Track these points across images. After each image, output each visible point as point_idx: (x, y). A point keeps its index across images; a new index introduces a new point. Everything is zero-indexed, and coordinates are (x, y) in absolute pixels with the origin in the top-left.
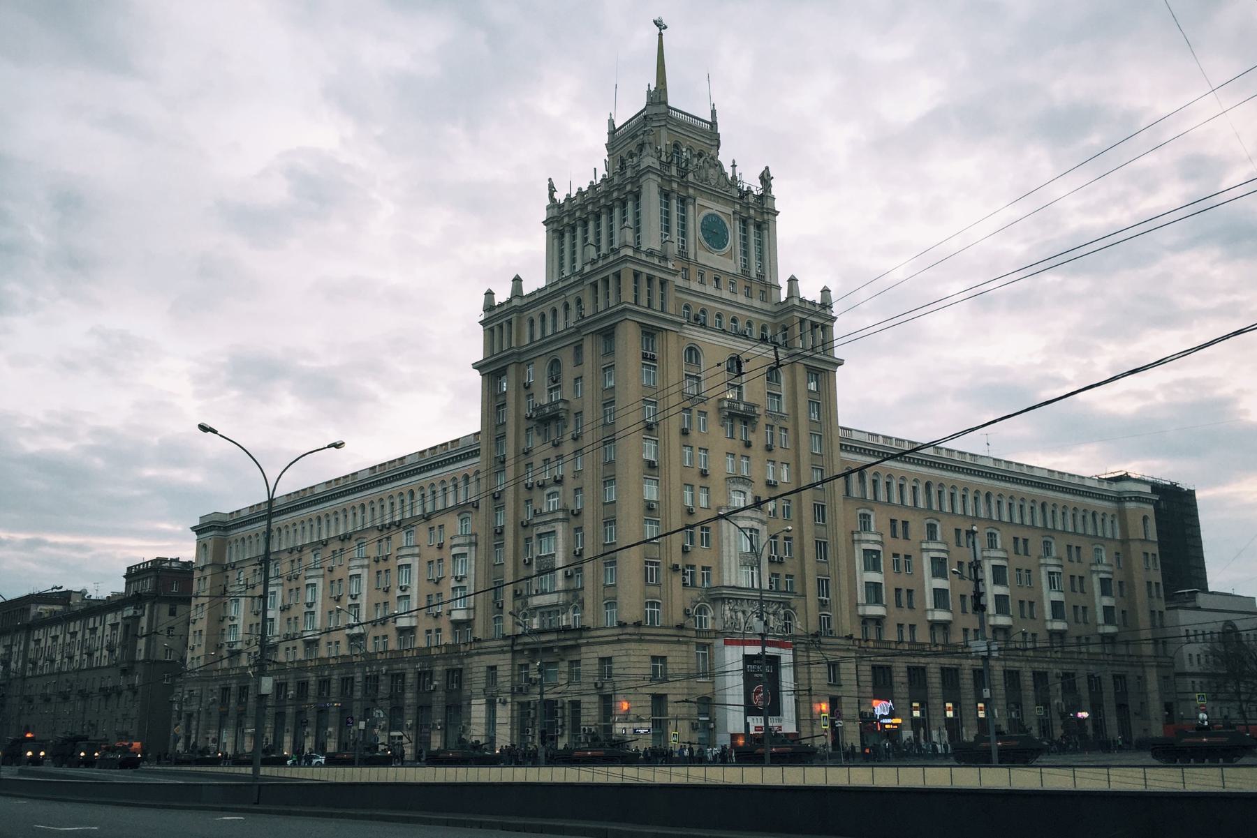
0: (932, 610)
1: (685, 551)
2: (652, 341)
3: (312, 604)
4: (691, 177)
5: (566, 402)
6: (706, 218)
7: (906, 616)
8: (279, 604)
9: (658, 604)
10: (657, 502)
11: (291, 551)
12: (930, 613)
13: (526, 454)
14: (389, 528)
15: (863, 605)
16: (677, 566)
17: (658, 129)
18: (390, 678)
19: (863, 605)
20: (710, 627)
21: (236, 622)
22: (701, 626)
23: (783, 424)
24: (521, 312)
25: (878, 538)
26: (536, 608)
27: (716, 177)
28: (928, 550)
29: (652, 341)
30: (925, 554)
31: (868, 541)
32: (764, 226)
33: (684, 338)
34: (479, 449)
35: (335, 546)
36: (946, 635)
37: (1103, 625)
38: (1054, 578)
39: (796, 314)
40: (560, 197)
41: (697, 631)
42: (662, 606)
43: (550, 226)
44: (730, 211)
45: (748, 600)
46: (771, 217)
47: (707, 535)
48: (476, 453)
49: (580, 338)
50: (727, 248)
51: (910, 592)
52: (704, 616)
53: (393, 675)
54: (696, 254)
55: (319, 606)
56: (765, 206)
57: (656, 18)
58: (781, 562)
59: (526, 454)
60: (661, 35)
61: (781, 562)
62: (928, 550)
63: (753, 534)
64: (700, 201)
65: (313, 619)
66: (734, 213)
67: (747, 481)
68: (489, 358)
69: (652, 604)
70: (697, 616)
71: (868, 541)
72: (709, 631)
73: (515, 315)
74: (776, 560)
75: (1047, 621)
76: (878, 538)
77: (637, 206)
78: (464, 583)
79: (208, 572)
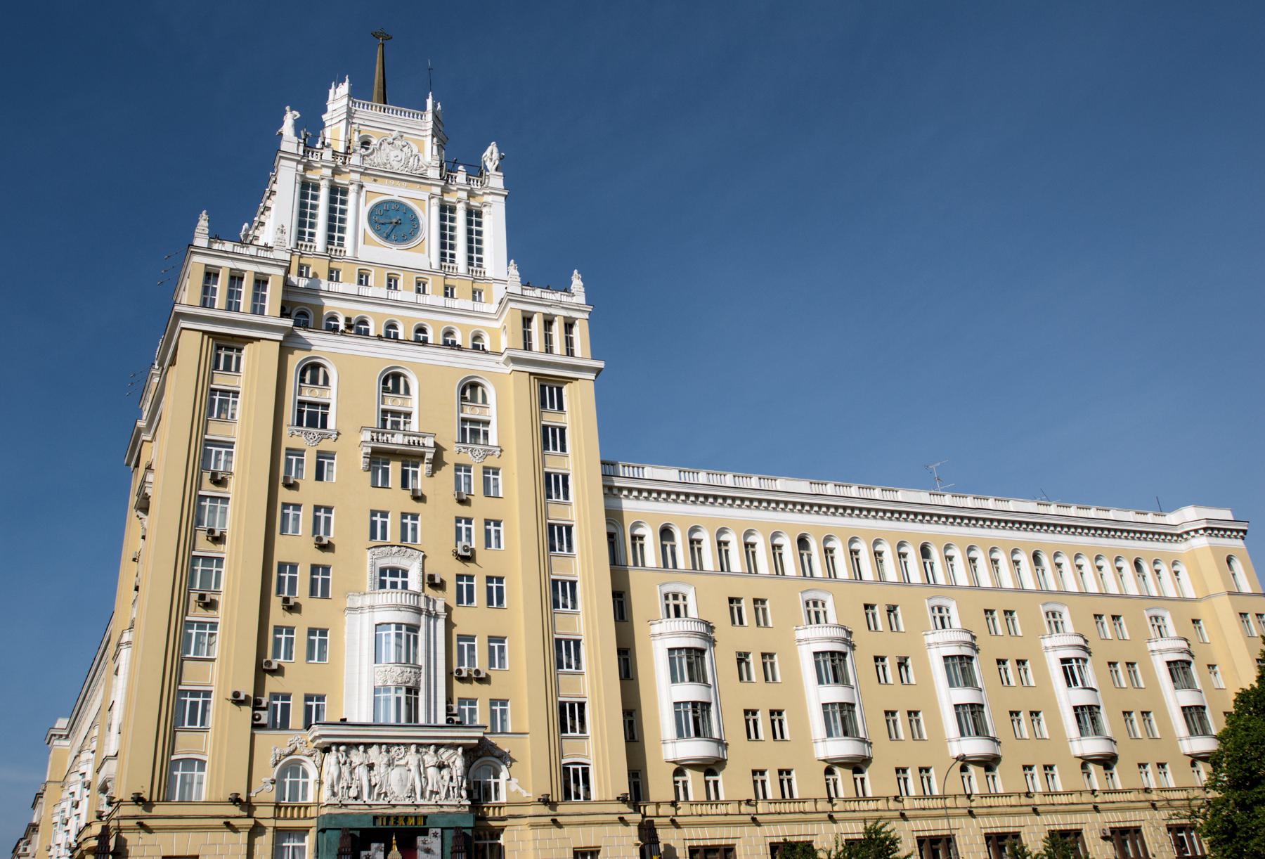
7: (768, 755)
20: (311, 798)
45: (380, 745)
51: (776, 713)
52: (301, 780)
64: (369, 185)
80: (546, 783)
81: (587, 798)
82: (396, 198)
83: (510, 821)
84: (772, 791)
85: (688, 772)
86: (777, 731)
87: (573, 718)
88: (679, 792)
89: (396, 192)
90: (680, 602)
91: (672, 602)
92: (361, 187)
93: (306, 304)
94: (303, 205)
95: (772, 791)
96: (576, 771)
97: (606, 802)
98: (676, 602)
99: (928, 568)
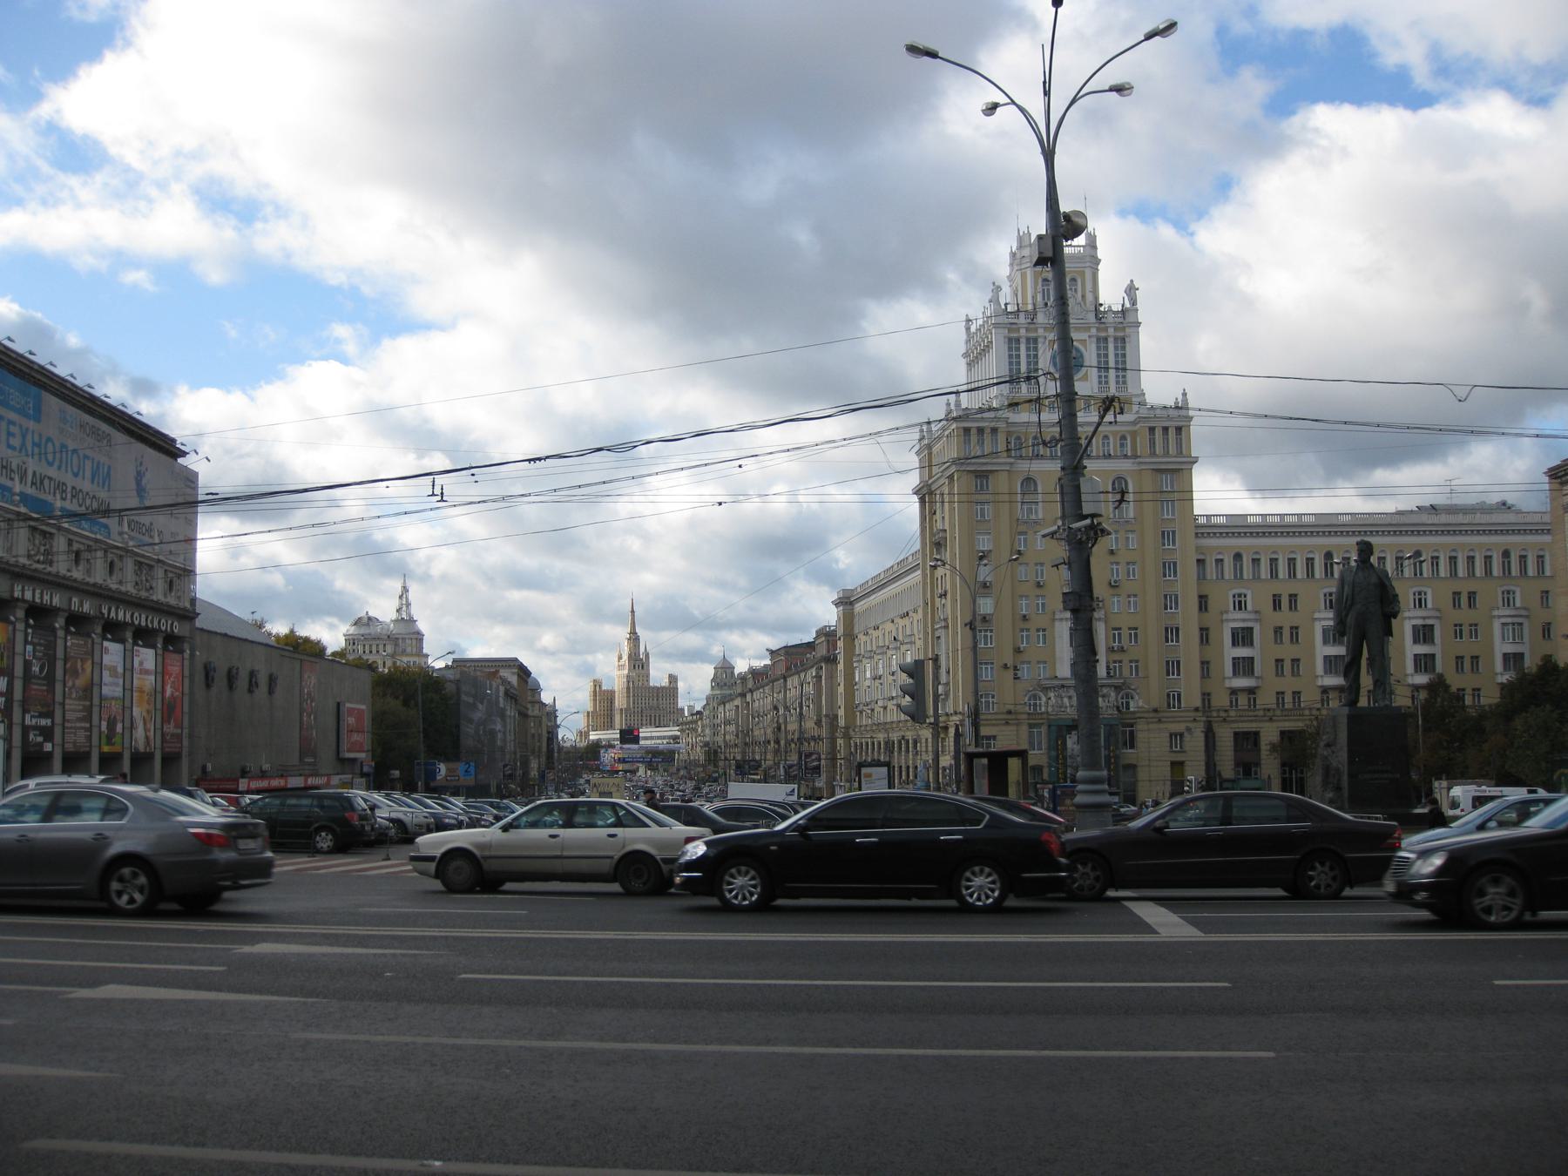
0: (1322, 676)
2: (987, 482)
15: (1229, 678)
16: (1006, 665)
19: (1229, 678)
22: (1035, 709)
25: (1252, 616)
28: (1320, 619)
29: (987, 482)
31: (1234, 620)
32: (1126, 339)
41: (1029, 714)
56: (1127, 321)
58: (1122, 650)
61: (1122, 650)
66: (1090, 337)
71: (1234, 620)
75: (1497, 674)
76: (1252, 616)
81: (1179, 708)
83: (1138, 720)
86: (1295, 672)
88: (1234, 704)
91: (1237, 599)
94: (1010, 356)
96: (1174, 695)
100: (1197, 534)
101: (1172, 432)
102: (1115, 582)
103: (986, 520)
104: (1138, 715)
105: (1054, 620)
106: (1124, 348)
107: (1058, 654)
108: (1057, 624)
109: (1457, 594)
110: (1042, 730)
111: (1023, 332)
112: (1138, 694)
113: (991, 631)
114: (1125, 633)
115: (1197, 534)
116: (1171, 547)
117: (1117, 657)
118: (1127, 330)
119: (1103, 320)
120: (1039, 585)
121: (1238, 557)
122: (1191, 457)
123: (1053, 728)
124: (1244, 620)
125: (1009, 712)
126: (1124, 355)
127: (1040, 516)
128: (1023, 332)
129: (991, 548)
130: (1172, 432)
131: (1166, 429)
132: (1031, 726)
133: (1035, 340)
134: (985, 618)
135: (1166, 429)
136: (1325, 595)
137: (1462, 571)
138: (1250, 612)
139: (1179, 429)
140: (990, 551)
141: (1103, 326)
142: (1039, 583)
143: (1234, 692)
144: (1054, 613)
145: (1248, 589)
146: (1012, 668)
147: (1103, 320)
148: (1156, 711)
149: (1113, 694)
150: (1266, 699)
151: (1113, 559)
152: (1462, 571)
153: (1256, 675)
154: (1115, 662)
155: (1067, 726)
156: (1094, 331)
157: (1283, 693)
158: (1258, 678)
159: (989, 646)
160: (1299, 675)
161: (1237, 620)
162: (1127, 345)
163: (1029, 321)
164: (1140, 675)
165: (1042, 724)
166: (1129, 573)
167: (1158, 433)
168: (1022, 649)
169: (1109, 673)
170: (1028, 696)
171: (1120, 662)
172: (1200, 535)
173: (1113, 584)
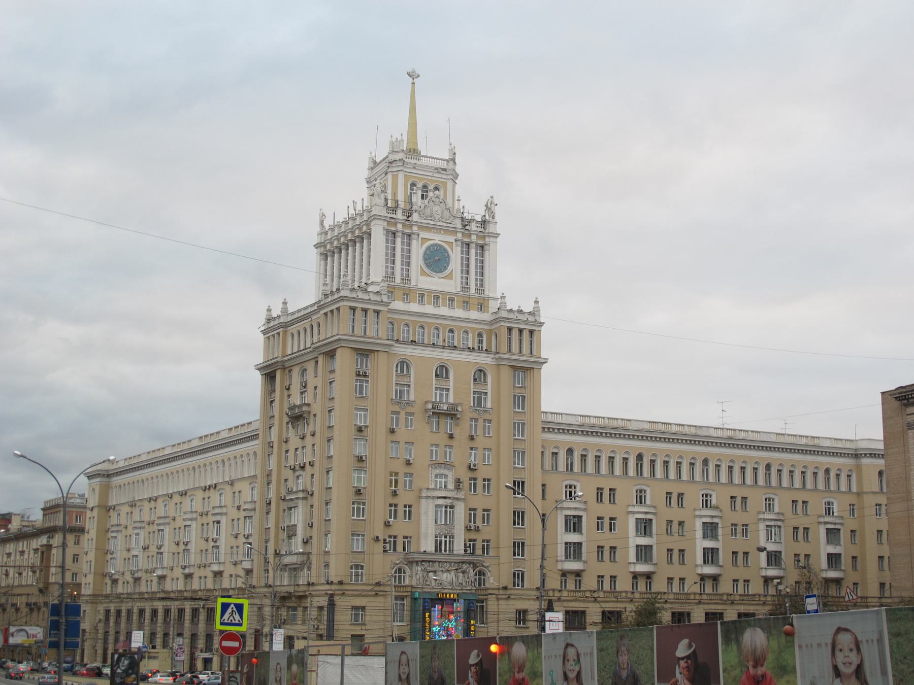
0: (634, 563)
1: (387, 525)
2: (367, 360)
3: (161, 546)
4: (415, 217)
5: (309, 405)
6: (428, 248)
7: (607, 569)
8: (142, 544)
9: (362, 567)
10: (364, 488)
11: (150, 500)
12: (632, 565)
13: (286, 442)
14: (209, 489)
16: (377, 537)
17: (396, 173)
18: (206, 610)
19: (561, 561)
20: (407, 582)
21: (114, 556)
23: (487, 417)
24: (287, 327)
25: (581, 506)
26: (286, 565)
27: (439, 212)
28: (633, 513)
29: (367, 360)
30: (630, 516)
31: (569, 508)
32: (486, 247)
33: (395, 354)
34: (258, 434)
35: (176, 498)
36: (649, 585)
37: (826, 571)
38: (771, 531)
39: (503, 324)
40: (328, 223)
42: (365, 568)
43: (319, 249)
44: (451, 239)
46: (492, 239)
47: (410, 511)
48: (255, 437)
49: (317, 356)
50: (447, 272)
53: (208, 609)
54: (417, 280)
55: (166, 550)
56: (487, 231)
57: (409, 70)
59: (286, 442)
60: (413, 83)
61: (477, 530)
62: (633, 513)
63: (448, 509)
64: (424, 235)
65: (162, 560)
66: (456, 240)
67: (448, 465)
68: (266, 362)
69: (357, 567)
70: (397, 575)
71: (569, 508)
72: (406, 586)
73: (281, 329)
74: (472, 528)
76: (581, 506)
77: (370, 244)
78: (250, 540)
79: (96, 511)
80: (506, 580)
81: (523, 586)
82: (437, 242)
83: (489, 596)
84: (607, 586)
85: (568, 575)
86: (613, 559)
87: (519, 549)
89: (437, 238)
90: (573, 490)
91: (568, 490)
92: (418, 235)
93: (393, 318)
95: (607, 586)
96: (518, 574)
97: (530, 589)
98: (570, 490)
99: (706, 472)
100: (544, 428)
101: (526, 334)
102: (475, 465)
103: (364, 398)
104: (490, 592)
105: (420, 497)
106: (482, 255)
107: (423, 530)
108: (423, 501)
109: (600, 491)
110: (405, 602)
111: (400, 226)
112: (490, 571)
113: (364, 504)
114: (479, 514)
115: (544, 428)
116: (520, 437)
117: (473, 536)
118: (487, 239)
119: (467, 227)
120: (408, 463)
121: (570, 451)
122: (540, 358)
123: (407, 602)
124: (835, 524)
125: (378, 584)
126: (482, 262)
127: (412, 398)
128: (400, 226)
129: (368, 424)
130: (526, 334)
131: (521, 331)
132: (397, 598)
133: (409, 235)
134: (359, 490)
135: (521, 331)
136: (637, 492)
137: (737, 479)
138: (836, 517)
139: (531, 332)
140: (367, 427)
141: (467, 232)
142: (409, 461)
143: (564, 574)
144: (421, 490)
145: (578, 481)
146: (382, 541)
147: (467, 227)
148: (505, 588)
149: (471, 570)
150: (589, 582)
151: (472, 444)
152: (737, 479)
153: (583, 559)
154: (470, 540)
155: (432, 599)
156: (459, 236)
157: (602, 577)
158: (584, 562)
159: (361, 518)
160: (615, 561)
161: (571, 508)
162: (486, 253)
163: (405, 218)
164: (491, 554)
165: (406, 596)
166: (484, 459)
167: (515, 333)
168: (391, 523)
169: (465, 551)
170: (395, 569)
171: (474, 540)
172: (546, 430)
173: (472, 467)
